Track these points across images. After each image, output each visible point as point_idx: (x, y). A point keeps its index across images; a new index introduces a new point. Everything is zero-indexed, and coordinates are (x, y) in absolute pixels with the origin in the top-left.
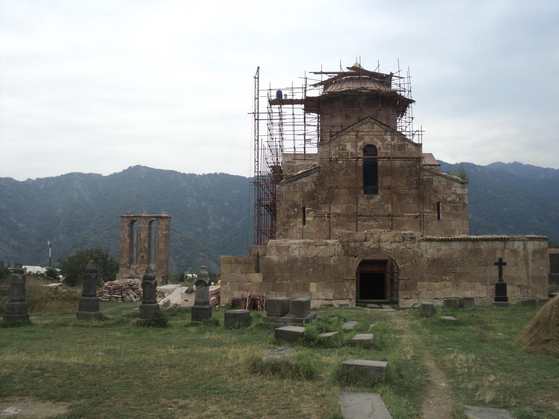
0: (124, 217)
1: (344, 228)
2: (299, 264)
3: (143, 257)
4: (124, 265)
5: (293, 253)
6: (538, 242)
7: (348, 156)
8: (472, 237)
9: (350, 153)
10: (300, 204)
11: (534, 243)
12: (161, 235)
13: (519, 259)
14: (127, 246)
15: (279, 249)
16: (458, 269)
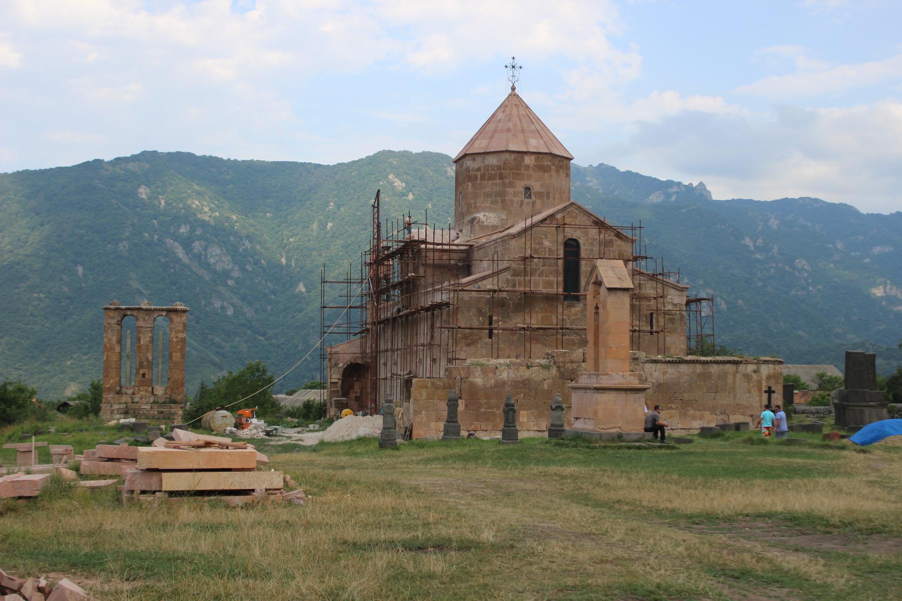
0: (110, 309)
1: (540, 343)
2: (507, 388)
3: (144, 375)
4: (109, 390)
5: (500, 375)
6: (773, 365)
7: (545, 252)
8: (703, 358)
9: (547, 249)
10: (486, 312)
11: (768, 367)
12: (175, 340)
13: (752, 384)
14: (115, 358)
15: (485, 370)
16: (686, 396)
